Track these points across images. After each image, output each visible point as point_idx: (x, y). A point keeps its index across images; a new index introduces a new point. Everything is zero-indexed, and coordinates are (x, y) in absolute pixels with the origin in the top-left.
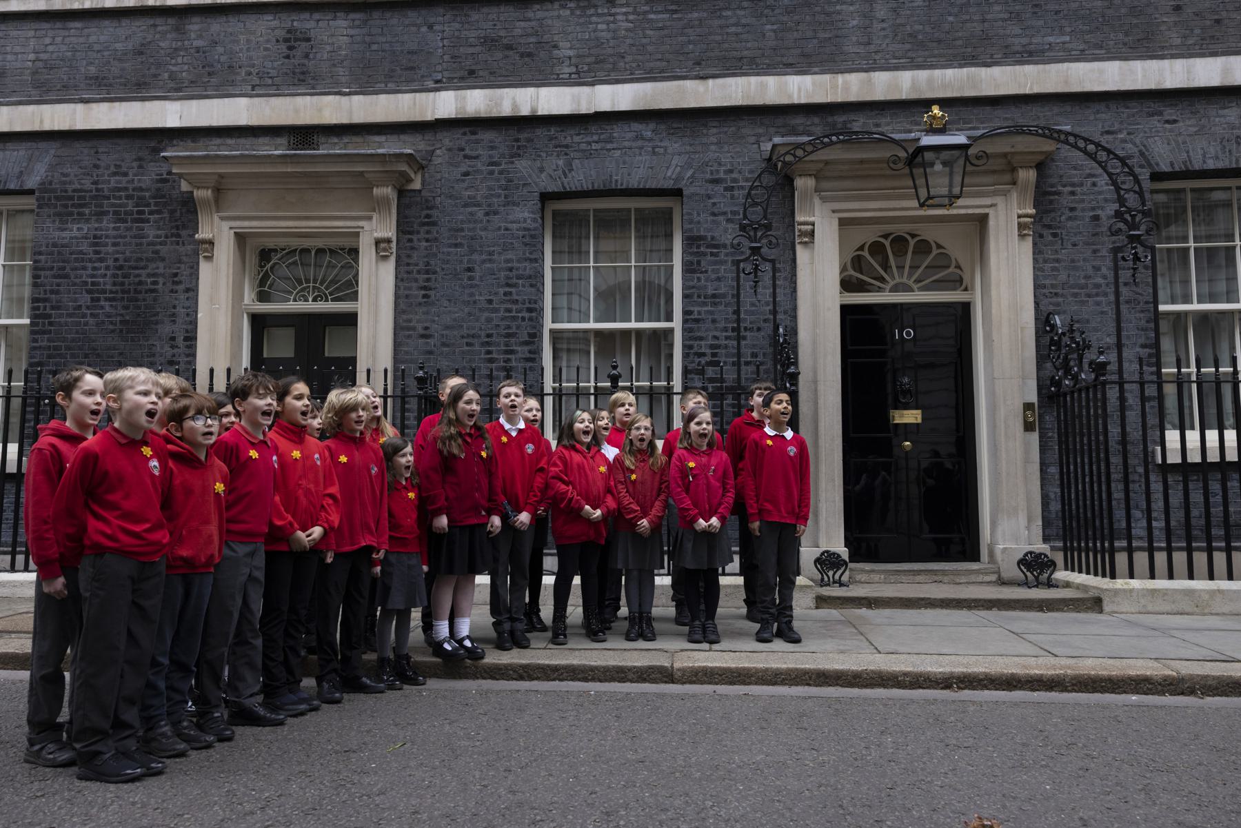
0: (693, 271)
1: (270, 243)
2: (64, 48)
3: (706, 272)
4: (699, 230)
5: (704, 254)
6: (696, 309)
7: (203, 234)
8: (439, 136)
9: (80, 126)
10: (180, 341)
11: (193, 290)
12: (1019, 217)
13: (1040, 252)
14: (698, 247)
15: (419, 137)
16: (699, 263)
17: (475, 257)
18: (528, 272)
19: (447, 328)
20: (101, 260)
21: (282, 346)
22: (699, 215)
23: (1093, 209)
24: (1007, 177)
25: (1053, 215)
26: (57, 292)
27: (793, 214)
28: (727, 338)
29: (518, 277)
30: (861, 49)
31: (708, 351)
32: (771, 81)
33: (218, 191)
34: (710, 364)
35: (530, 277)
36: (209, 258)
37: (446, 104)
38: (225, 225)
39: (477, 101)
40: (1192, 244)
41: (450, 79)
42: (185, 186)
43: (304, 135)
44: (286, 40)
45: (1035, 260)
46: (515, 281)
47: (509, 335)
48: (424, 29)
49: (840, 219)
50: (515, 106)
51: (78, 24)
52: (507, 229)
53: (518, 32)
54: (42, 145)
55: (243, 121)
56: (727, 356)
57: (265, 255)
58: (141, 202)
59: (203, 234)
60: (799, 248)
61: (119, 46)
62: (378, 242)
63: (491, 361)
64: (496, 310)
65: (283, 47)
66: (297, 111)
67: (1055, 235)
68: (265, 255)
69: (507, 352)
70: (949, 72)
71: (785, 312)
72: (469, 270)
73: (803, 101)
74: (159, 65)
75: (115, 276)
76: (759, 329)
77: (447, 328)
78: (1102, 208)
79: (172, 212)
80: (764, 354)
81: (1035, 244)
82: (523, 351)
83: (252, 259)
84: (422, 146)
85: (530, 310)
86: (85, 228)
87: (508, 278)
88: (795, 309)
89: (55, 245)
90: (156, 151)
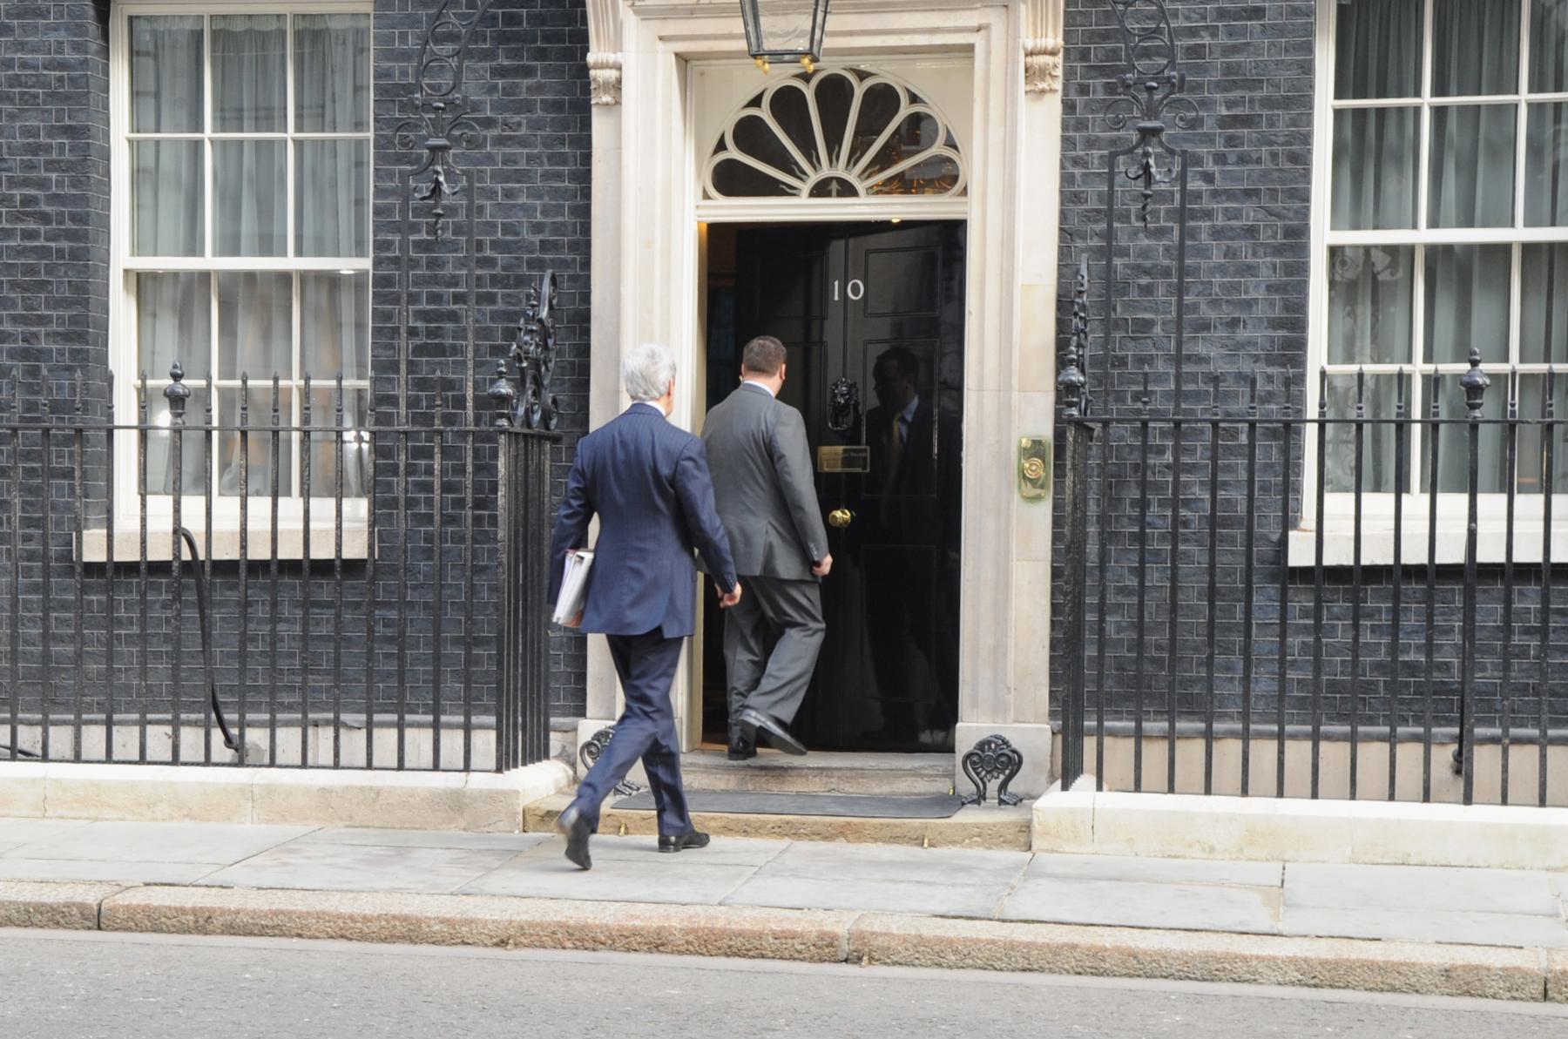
13: (1081, 125)
18: (67, 156)
23: (1193, 32)
28: (458, 298)
29: (51, 166)
31: (419, 324)
35: (71, 166)
45: (1067, 142)
46: (43, 174)
49: (677, 55)
52: (24, 65)
60: (594, 110)
67: (1110, 89)
78: (1213, 31)
81: (1068, 107)
87: (31, 167)
88: (588, 244)
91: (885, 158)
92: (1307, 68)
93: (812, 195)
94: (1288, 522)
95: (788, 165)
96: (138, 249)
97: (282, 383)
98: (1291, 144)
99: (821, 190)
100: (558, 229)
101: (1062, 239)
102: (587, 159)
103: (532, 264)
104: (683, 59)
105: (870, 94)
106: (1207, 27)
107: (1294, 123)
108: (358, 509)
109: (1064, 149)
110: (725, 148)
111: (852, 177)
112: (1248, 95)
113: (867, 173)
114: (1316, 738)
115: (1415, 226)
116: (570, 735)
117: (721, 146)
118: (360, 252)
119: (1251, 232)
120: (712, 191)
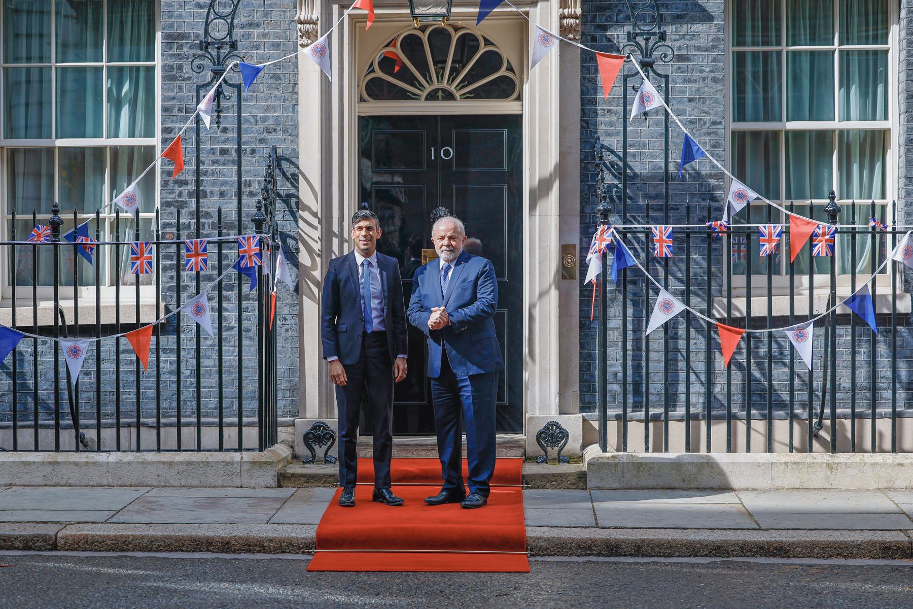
0: (173, 78)
3: (189, 79)
4: (180, 26)
5: (187, 57)
6: (177, 125)
12: (563, 17)
14: (180, 47)
16: (180, 68)
22: (181, 6)
25: (608, 13)
28: (214, 162)
34: (190, 195)
40: (785, 48)
56: (213, 184)
71: (285, 131)
76: (253, 151)
80: (259, 183)
88: (296, 128)
91: (471, 78)
93: (427, 99)
95: (412, 81)
97: (101, 215)
98: (712, 71)
99: (432, 96)
100: (277, 120)
101: (582, 127)
103: (261, 141)
106: (663, 5)
107: (714, 60)
109: (582, 72)
110: (373, 71)
111: (452, 88)
112: (687, 43)
113: (461, 86)
115: (780, 120)
116: (290, 429)
118: (149, 133)
119: (691, 122)
120: (366, 96)
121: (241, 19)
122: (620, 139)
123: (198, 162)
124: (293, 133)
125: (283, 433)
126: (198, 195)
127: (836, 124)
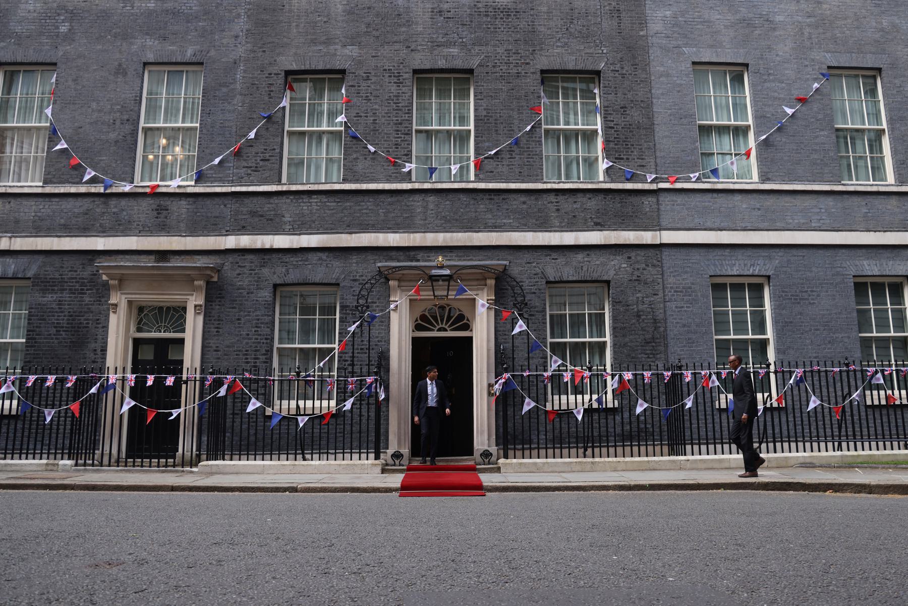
1: (144, 304)
2: (49, 211)
7: (113, 301)
8: (227, 256)
9: (55, 248)
10: (99, 352)
11: (106, 327)
15: (217, 257)
17: (242, 313)
19: (228, 347)
20: (62, 312)
21: (148, 354)
24: (483, 282)
26: (40, 327)
27: (389, 296)
30: (422, 222)
32: (381, 236)
33: (120, 280)
36: (115, 312)
37: (231, 242)
38: (123, 297)
39: (245, 241)
41: (234, 230)
42: (104, 278)
43: (163, 255)
44: (157, 210)
47: (256, 351)
48: (222, 206)
50: (263, 244)
51: (57, 200)
53: (266, 209)
54: (36, 257)
55: (134, 248)
57: (141, 309)
58: (83, 284)
59: (113, 301)
61: (76, 210)
62: (196, 306)
63: (248, 363)
64: (251, 339)
65: (155, 213)
66: (160, 243)
68: (141, 309)
69: (255, 359)
70: (460, 234)
72: (239, 319)
73: (395, 245)
74: (95, 220)
75: (68, 320)
77: (228, 347)
79: (98, 290)
82: (263, 358)
83: (135, 311)
84: (219, 261)
85: (266, 339)
86: (55, 296)
89: (39, 304)
90: (92, 261)
92: (545, 304)
94: (546, 401)
96: (280, 343)
99: (439, 330)
102: (389, 321)
104: (410, 300)
105: (450, 309)
108: (333, 403)
113: (449, 326)
114: (554, 448)
117: (417, 320)
121: (369, 300)
122: (511, 345)
123: (353, 353)
124: (388, 342)
125: (382, 456)
126: (353, 365)
127: (588, 339)
